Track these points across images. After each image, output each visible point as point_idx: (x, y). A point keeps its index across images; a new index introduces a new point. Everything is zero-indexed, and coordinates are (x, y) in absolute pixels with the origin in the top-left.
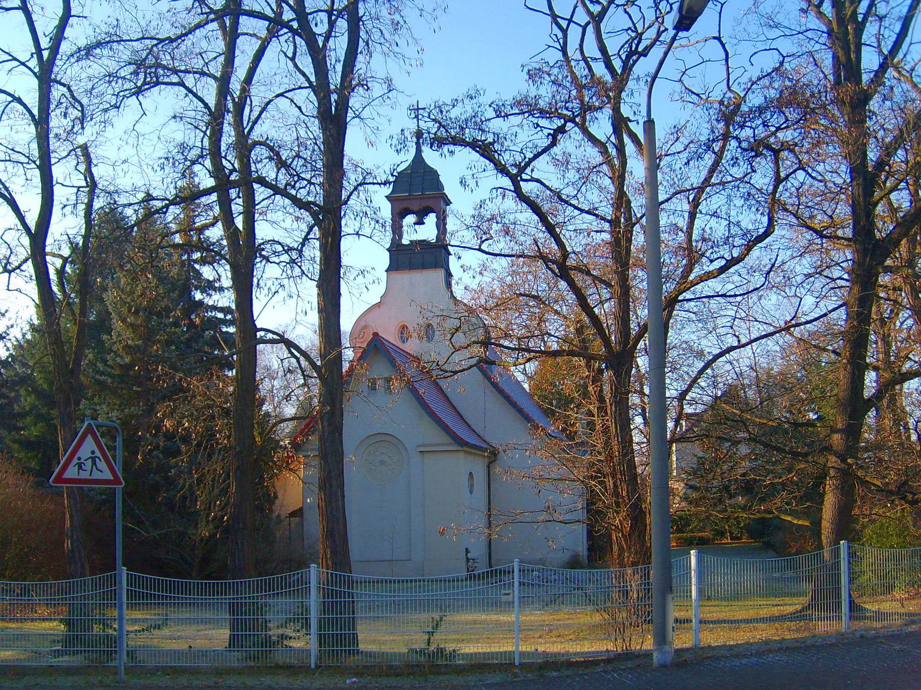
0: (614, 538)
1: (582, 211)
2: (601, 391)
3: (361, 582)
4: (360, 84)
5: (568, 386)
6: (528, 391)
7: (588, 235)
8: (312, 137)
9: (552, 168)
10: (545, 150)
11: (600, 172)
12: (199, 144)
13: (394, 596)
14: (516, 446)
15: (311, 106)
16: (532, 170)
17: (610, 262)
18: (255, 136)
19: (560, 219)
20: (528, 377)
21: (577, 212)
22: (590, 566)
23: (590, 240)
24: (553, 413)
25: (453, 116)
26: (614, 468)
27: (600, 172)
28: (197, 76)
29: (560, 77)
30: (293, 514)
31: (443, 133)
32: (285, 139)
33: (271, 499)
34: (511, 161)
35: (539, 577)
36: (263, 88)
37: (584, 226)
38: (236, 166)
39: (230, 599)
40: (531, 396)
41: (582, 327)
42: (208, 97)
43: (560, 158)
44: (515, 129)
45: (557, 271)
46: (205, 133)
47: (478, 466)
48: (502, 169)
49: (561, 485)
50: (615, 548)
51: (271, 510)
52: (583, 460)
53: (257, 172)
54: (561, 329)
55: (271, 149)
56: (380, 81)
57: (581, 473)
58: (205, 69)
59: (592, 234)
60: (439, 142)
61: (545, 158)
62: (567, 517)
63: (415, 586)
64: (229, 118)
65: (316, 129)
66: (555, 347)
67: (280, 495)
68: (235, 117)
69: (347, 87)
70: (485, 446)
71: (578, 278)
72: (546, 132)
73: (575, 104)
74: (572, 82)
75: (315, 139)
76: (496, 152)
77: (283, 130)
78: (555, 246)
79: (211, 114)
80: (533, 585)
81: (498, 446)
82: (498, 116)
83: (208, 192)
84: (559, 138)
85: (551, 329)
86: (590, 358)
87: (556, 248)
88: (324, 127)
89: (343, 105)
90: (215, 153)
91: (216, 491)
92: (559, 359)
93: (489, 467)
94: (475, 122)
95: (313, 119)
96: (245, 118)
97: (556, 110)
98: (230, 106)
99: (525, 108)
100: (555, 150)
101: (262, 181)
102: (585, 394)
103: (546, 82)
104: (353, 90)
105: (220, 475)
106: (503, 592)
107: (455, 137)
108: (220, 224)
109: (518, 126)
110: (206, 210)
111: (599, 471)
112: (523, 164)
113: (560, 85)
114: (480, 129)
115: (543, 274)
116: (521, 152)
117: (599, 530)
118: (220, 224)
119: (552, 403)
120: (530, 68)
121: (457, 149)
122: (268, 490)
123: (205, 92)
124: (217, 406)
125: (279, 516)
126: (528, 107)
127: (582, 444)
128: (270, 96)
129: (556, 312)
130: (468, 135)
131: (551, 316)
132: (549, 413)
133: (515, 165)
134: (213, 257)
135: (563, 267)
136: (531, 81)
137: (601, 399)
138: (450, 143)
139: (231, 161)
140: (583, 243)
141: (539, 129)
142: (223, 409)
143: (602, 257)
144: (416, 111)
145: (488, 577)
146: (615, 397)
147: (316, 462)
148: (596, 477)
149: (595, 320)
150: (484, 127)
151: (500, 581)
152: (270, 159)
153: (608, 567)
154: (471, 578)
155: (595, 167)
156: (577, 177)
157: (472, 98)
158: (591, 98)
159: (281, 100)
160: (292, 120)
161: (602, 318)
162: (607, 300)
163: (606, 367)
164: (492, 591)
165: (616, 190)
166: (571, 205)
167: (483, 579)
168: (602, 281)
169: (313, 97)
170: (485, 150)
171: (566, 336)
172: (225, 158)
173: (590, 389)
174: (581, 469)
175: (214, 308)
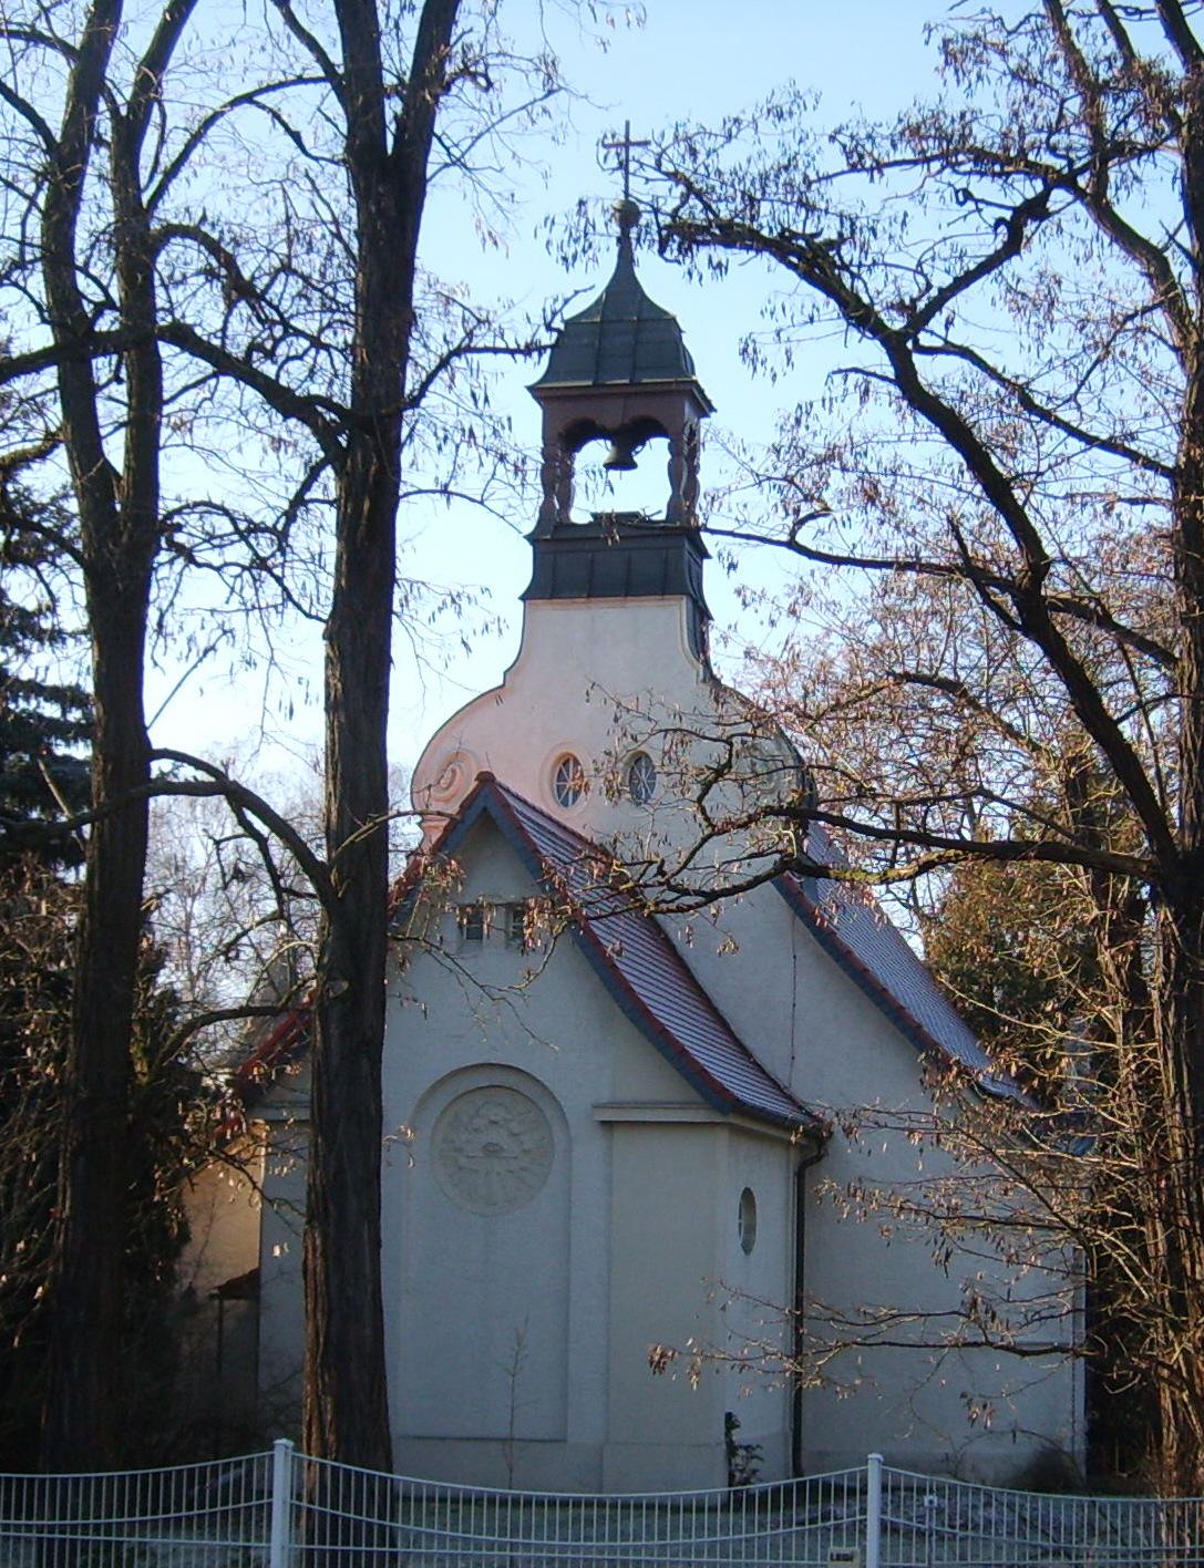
0: (1167, 1403)
1: (1091, 441)
2: (1137, 964)
3: (419, 1500)
4: (466, 72)
5: (1039, 948)
6: (921, 956)
7: (1108, 511)
8: (327, 217)
9: (1004, 317)
10: (990, 265)
11: (1143, 330)
12: (16, 232)
13: (514, 1546)
14: (882, 1118)
15: (329, 130)
16: (949, 323)
17: (1168, 591)
18: (169, 211)
19: (1026, 463)
20: (923, 918)
21: (1075, 445)
22: (1093, 1488)
23: (1111, 524)
24: (993, 1025)
25: (725, 166)
26: (1171, 1196)
27: (1143, 330)
28: (19, 44)
29: (1035, 61)
30: (233, 1289)
31: (695, 211)
32: (252, 220)
33: (169, 1239)
34: (889, 295)
35: (940, 1511)
36: (197, 81)
37: (1096, 486)
38: (115, 293)
39: (40, 1529)
40: (929, 971)
41: (1083, 775)
42: (47, 102)
43: (1030, 289)
44: (904, 205)
45: (1014, 612)
46: (32, 200)
47: (770, 1178)
48: (860, 316)
49: (1011, 1239)
50: (1170, 1436)
51: (170, 1277)
52: (1078, 1168)
53: (171, 311)
54: (1021, 780)
55: (213, 247)
56: (524, 65)
57: (1071, 1206)
58: (41, 26)
59: (1119, 507)
60: (683, 236)
61: (985, 286)
62: (1030, 1336)
63: (576, 1520)
64: (100, 160)
65: (341, 194)
66: (1003, 831)
67: (196, 1230)
68: (116, 158)
69: (429, 79)
70: (788, 1112)
71: (1077, 635)
72: (992, 214)
73: (1079, 138)
74: (1068, 76)
75: (335, 221)
76: (845, 267)
77: (249, 196)
78: (1007, 540)
79: (51, 147)
80: (921, 1534)
81: (829, 1116)
82: (853, 168)
83: (32, 363)
84: (1027, 231)
85: (994, 780)
86: (1104, 869)
87: (1013, 544)
88: (362, 190)
89: (418, 129)
90: (58, 257)
91: (17, 1211)
92: (1013, 869)
93: (800, 1175)
94: (789, 184)
95: (331, 168)
96: (146, 162)
97: (1022, 153)
98: (105, 126)
99: (932, 147)
100: (1014, 266)
101: (183, 337)
102: (1089, 973)
103: (994, 75)
104: (447, 88)
105: (31, 1166)
106: (833, 1549)
107: (730, 223)
108: (61, 455)
109: (912, 196)
110: (26, 415)
111: (1125, 1202)
112: (921, 305)
113: (1033, 83)
114: (801, 203)
115: (974, 618)
116: (918, 270)
117: (1123, 1380)
118: (61, 455)
119: (993, 993)
120: (950, 34)
121: (735, 257)
122: (163, 1216)
123: (39, 87)
124: (31, 969)
125: (191, 1291)
126: (943, 145)
127: (1078, 1119)
128: (216, 101)
129: (1010, 731)
130: (768, 219)
131: (993, 743)
132: (980, 1025)
133: (900, 307)
134: (39, 545)
135: (1029, 602)
136: (950, 72)
137: (1136, 989)
138: (716, 241)
139: (99, 279)
140: (1092, 532)
141: (970, 205)
142: (46, 975)
143: (1146, 574)
144: (622, 149)
145: (788, 1504)
146: (1178, 985)
147: (301, 1141)
148: (1118, 1220)
149: (1122, 758)
150: (812, 196)
151: (825, 1518)
152: (210, 274)
153: (1145, 1490)
154: (738, 1502)
155: (1130, 318)
156: (1078, 345)
157: (780, 116)
158: (1124, 121)
159: (246, 110)
160: (275, 170)
161: (1144, 752)
162: (1157, 701)
163: (1152, 894)
164: (800, 1546)
165: (1191, 382)
166: (1059, 423)
167: (776, 1508)
168: (1145, 646)
169: (334, 107)
170: (816, 263)
171: (1036, 801)
172: (85, 270)
173: (1105, 957)
174: (1073, 1195)
175: (34, 689)
